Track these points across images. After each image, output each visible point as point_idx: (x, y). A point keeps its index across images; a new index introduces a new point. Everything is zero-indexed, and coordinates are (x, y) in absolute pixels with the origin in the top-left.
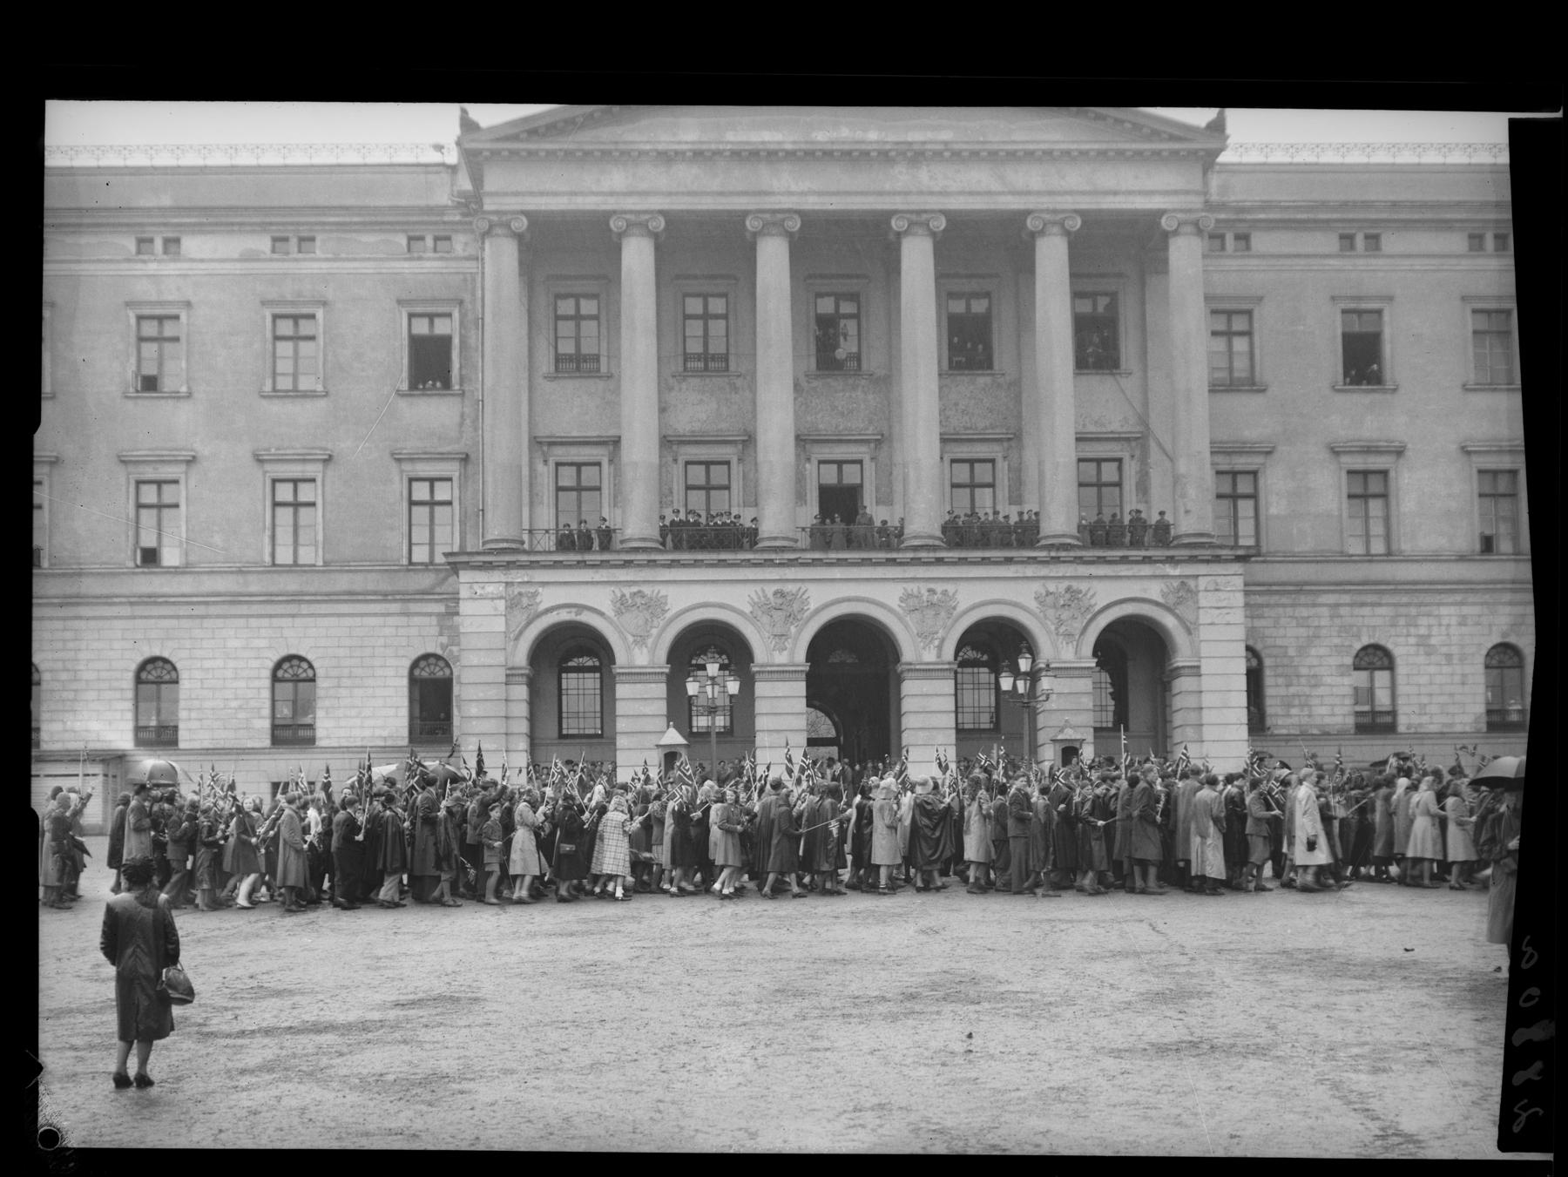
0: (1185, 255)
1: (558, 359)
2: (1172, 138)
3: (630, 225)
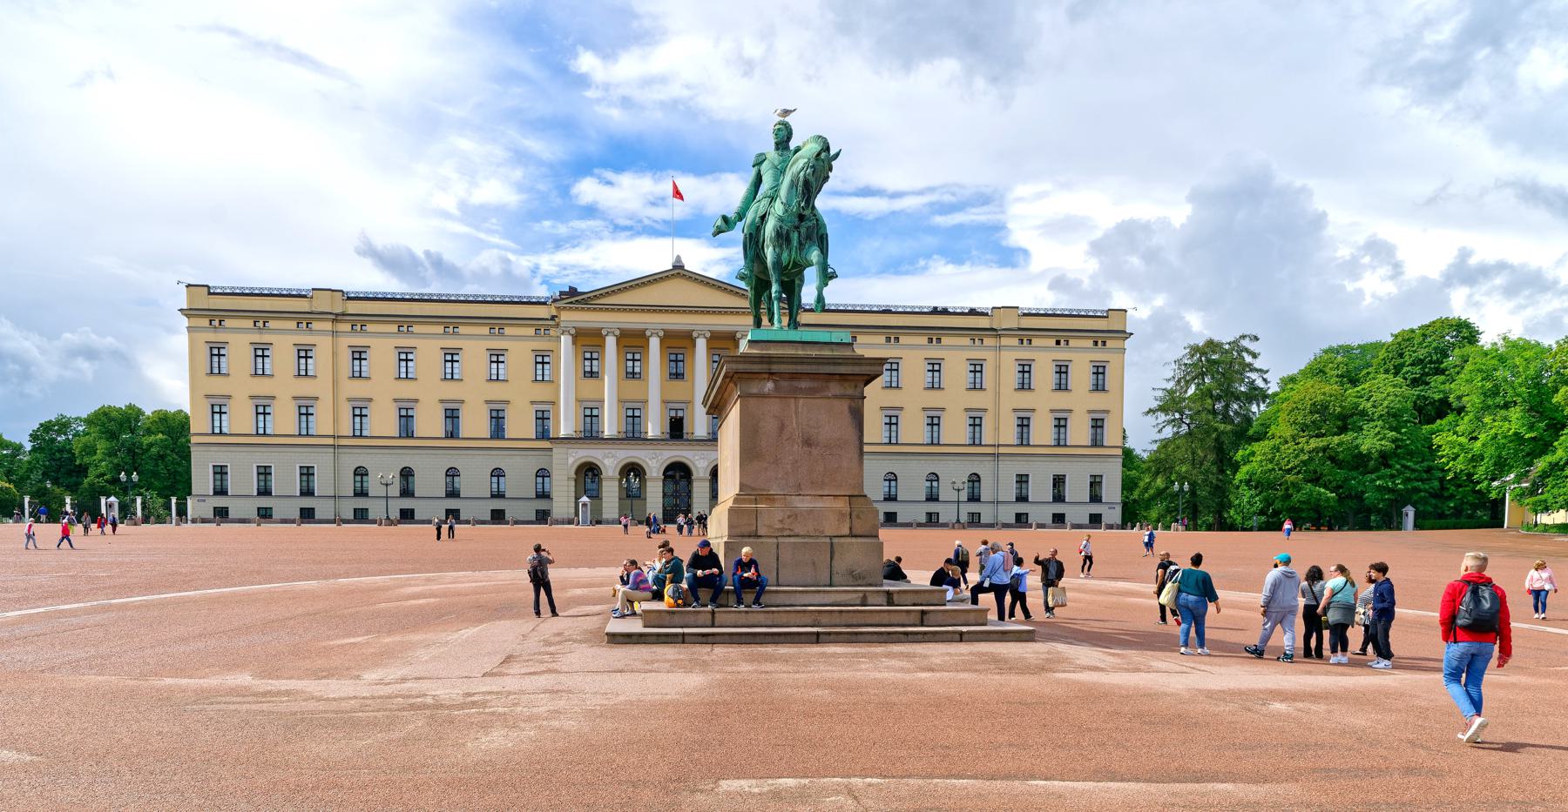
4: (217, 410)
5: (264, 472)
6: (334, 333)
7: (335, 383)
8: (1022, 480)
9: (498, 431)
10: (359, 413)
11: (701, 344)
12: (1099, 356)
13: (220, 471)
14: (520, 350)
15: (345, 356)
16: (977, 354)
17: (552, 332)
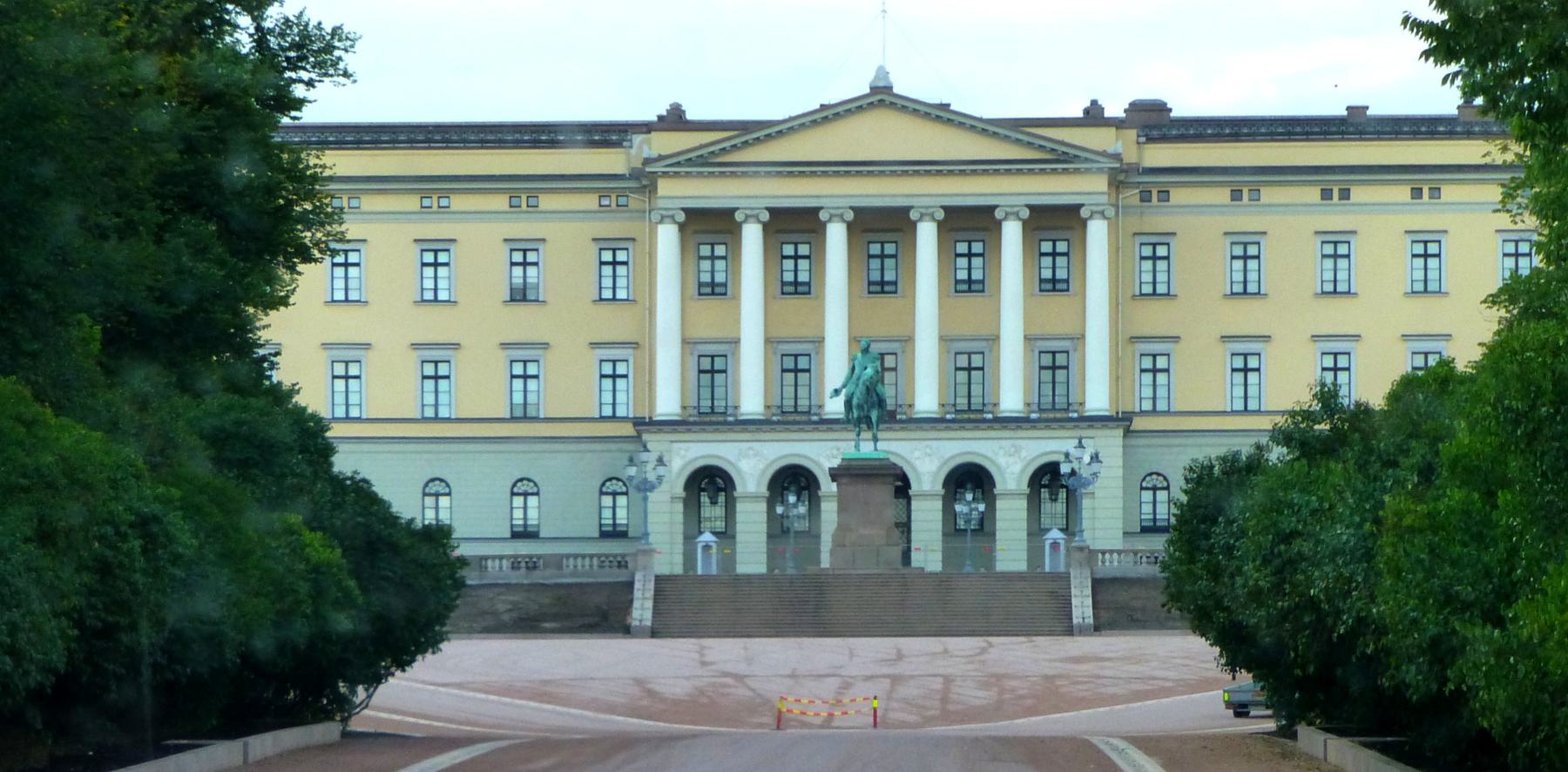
0: (1097, 232)
1: (700, 285)
2: (1086, 160)
3: (747, 217)
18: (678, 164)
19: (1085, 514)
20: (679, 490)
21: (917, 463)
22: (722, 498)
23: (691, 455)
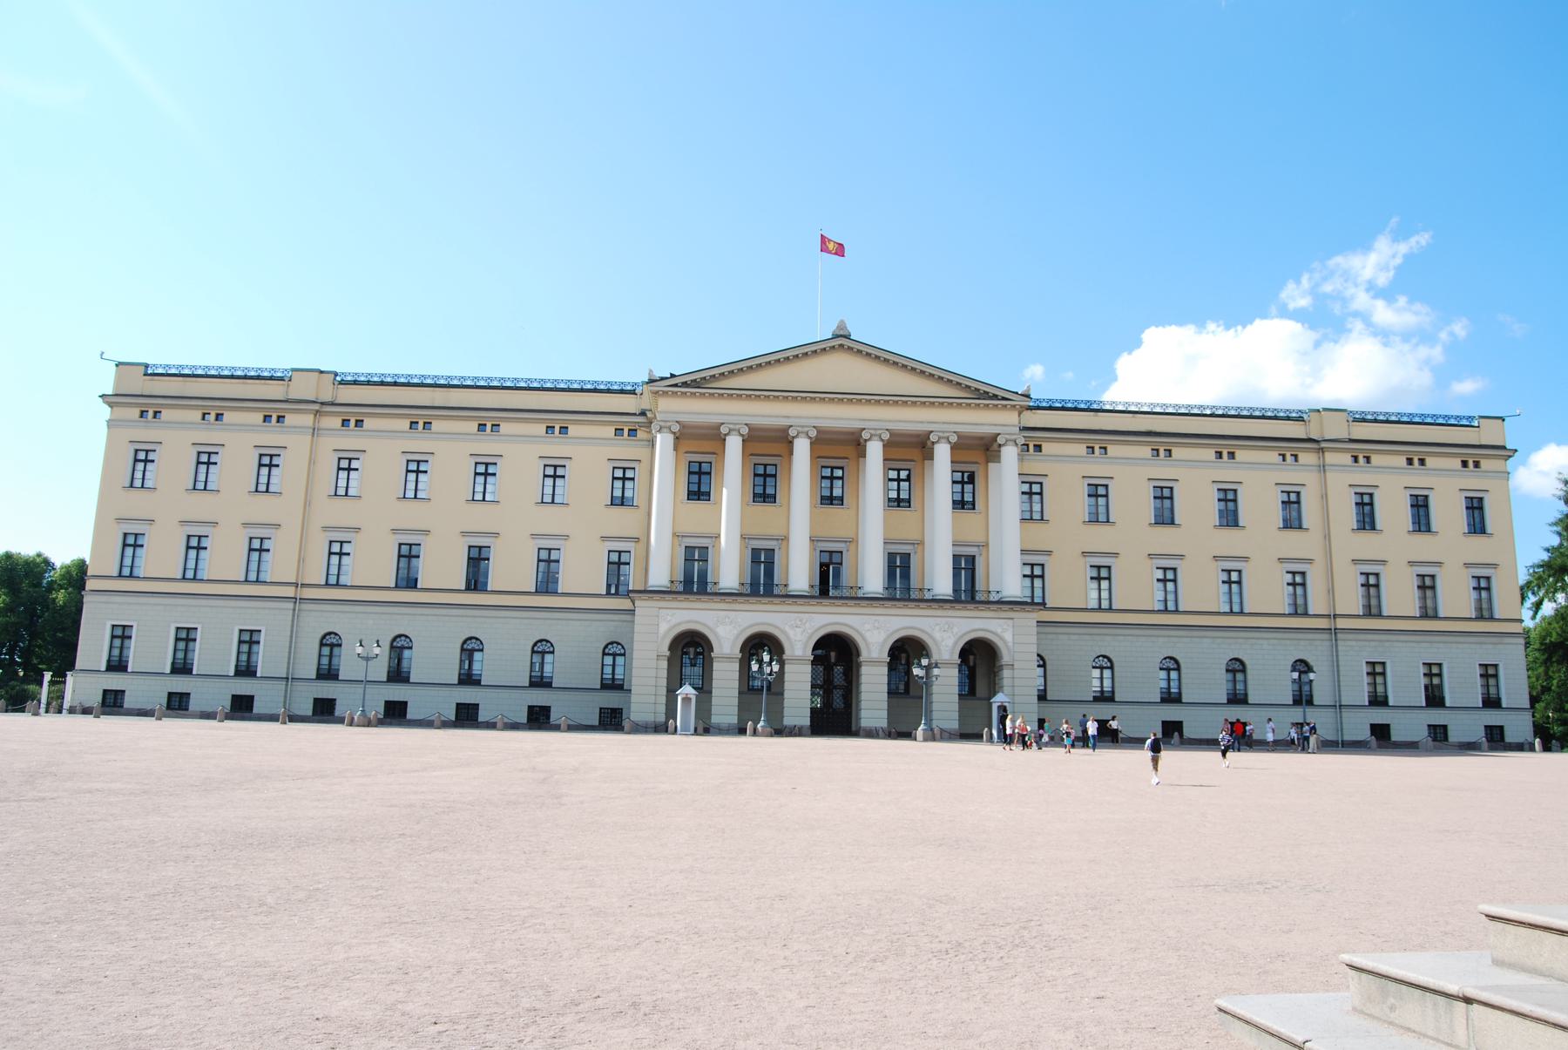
0: (1009, 454)
4: (131, 543)
5: (186, 637)
6: (315, 431)
7: (307, 503)
8: (1376, 671)
9: (547, 583)
10: (338, 551)
11: (875, 451)
12: (1473, 481)
13: (121, 635)
14: (591, 456)
15: (328, 464)
16: (1291, 476)
17: (641, 434)
18: (676, 385)
19: (1006, 682)
20: (665, 650)
21: (868, 635)
22: (699, 661)
23: (674, 621)
